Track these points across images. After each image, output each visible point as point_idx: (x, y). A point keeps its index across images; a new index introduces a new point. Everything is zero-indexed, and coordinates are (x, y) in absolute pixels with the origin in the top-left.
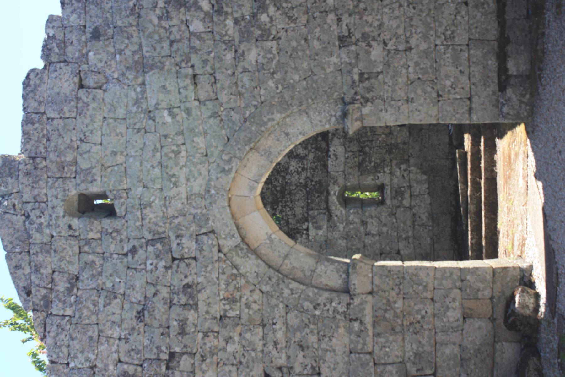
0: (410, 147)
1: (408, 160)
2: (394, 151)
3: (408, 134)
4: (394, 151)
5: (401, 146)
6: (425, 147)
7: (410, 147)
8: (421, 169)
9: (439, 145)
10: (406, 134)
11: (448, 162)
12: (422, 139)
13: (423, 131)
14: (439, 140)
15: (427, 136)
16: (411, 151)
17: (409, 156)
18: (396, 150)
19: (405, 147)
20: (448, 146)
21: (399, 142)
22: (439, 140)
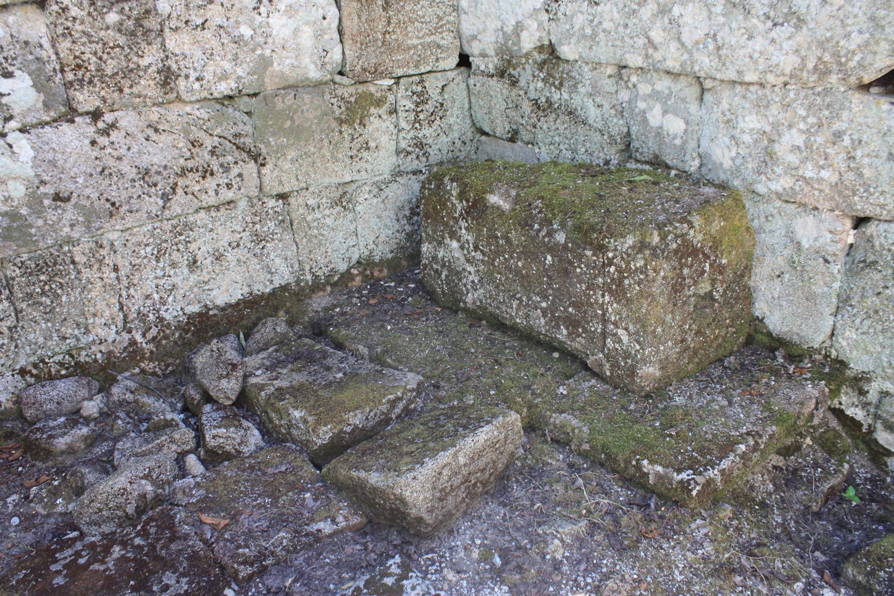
0: (154, 115)
1: (70, 114)
2: (112, 18)
3: (224, 88)
4: (112, 18)
5: (151, 57)
6: (166, 198)
7: (154, 115)
8: (34, 201)
9: (193, 264)
10: (224, 77)
11: (112, 335)
12: (208, 172)
13: (252, 166)
14: (218, 257)
15: (229, 195)
16: (127, 120)
17: (96, 115)
18: (119, 28)
19: (148, 86)
20: (195, 308)
21: (172, 42)
22: (218, 257)
